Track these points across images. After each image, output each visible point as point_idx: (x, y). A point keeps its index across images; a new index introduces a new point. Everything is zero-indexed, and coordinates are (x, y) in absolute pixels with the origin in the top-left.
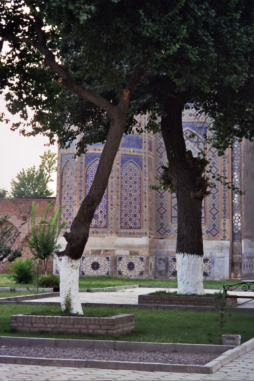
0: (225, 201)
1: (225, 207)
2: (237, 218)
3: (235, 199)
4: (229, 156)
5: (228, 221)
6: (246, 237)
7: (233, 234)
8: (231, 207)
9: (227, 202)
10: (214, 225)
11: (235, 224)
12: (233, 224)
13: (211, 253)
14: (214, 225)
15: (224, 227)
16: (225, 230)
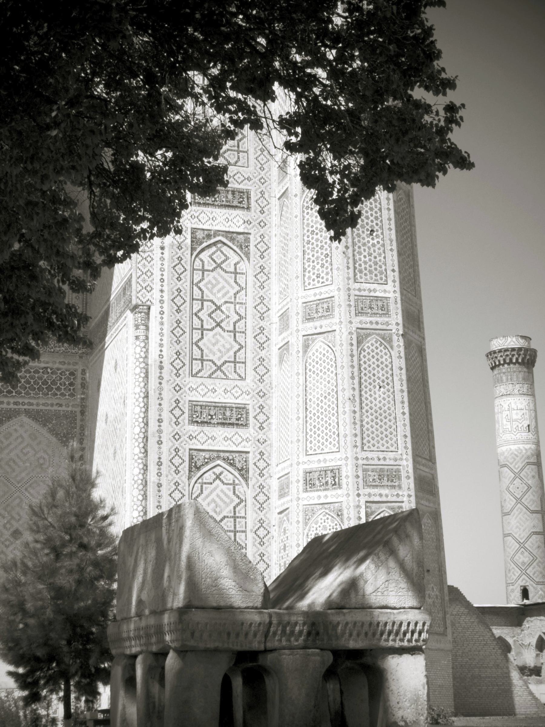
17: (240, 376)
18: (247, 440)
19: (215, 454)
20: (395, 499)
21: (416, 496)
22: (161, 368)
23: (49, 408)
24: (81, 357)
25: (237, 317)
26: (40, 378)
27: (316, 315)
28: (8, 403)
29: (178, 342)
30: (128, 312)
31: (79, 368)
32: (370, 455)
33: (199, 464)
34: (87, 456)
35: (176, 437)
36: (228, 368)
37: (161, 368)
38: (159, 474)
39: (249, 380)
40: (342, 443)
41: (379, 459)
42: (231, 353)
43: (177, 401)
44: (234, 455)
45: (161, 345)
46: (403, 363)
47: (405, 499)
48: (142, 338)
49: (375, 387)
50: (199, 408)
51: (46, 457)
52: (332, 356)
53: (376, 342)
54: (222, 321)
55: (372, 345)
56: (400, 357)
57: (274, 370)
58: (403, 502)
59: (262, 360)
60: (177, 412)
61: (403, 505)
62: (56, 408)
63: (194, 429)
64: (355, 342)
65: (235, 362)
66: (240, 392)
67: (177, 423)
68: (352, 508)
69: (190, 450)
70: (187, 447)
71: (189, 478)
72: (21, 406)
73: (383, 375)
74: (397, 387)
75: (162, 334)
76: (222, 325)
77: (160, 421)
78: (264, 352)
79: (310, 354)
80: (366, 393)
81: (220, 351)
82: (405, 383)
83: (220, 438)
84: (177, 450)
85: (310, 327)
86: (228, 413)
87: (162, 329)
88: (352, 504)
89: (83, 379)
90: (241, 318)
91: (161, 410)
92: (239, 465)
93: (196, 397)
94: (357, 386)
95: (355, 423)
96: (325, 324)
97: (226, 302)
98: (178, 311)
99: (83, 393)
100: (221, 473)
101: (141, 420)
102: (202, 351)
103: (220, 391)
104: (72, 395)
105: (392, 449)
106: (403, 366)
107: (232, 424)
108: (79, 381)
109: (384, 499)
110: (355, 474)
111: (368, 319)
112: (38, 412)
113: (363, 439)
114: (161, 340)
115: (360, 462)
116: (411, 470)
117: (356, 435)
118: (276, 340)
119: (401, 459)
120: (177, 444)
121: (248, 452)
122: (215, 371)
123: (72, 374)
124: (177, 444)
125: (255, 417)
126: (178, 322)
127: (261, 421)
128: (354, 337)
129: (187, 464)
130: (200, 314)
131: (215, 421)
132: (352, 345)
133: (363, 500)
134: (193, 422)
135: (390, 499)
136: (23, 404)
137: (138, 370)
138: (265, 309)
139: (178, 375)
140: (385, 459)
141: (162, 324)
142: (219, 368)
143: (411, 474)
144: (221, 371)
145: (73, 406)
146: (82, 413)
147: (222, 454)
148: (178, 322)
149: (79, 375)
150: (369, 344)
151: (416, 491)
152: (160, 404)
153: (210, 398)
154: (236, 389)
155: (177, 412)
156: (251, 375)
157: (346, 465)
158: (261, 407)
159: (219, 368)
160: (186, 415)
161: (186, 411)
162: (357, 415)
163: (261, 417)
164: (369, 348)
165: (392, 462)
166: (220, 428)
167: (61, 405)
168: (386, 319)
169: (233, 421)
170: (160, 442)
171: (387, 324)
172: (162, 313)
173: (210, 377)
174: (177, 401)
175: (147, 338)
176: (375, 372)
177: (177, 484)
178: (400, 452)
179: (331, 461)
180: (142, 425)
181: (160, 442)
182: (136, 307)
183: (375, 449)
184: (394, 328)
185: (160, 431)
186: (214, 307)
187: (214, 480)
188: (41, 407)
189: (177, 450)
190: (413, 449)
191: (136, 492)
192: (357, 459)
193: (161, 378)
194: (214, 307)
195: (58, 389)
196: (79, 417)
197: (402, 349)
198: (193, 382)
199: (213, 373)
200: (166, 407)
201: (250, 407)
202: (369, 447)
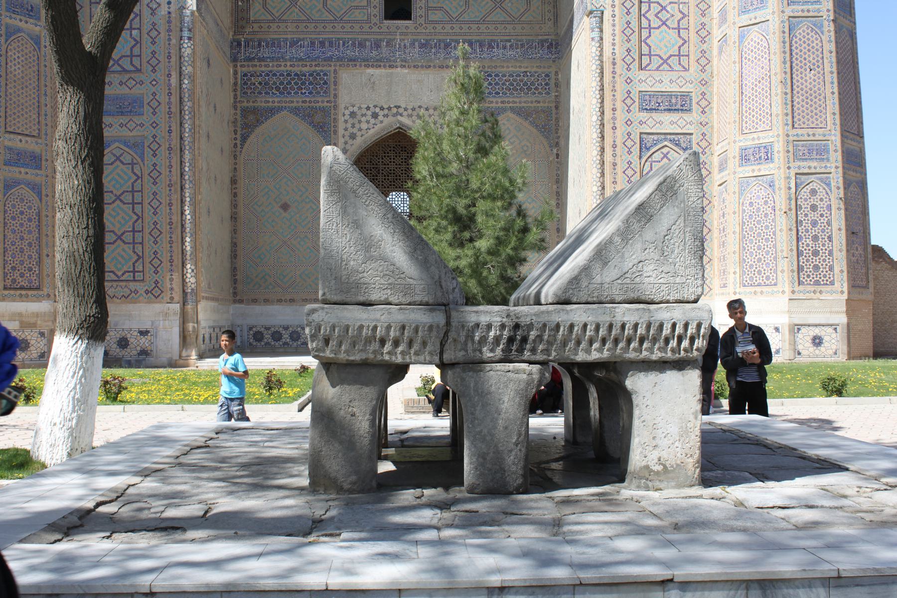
0: (171, 247)
1: (171, 256)
2: (189, 271)
3: (187, 244)
4: (176, 183)
5: (176, 276)
6: (207, 298)
7: (184, 293)
8: (180, 256)
9: (174, 248)
10: (156, 282)
11: (187, 280)
12: (184, 280)
13: (153, 322)
14: (156, 282)
15: (171, 284)
16: (172, 289)
17: (683, 67)
18: (691, 123)
19: (663, 137)
20: (823, 170)
21: (844, 167)
22: (614, 64)
23: (530, 105)
24: (554, 61)
25: (681, 16)
26: (521, 81)
27: (751, 8)
28: (497, 103)
29: (628, 41)
30: (585, 17)
31: (553, 70)
32: (800, 132)
33: (648, 145)
34: (562, 143)
35: (629, 122)
36: (674, 61)
37: (614, 64)
38: (614, 155)
39: (692, 70)
40: (774, 122)
41: (809, 136)
42: (676, 48)
43: (629, 92)
44: (679, 137)
45: (614, 44)
46: (833, 47)
47: (833, 170)
48: (597, 39)
49: (806, 70)
50: (647, 97)
51: (529, 144)
52: (766, 44)
53: (808, 29)
54: (667, 20)
55: (804, 31)
56: (830, 41)
57: (715, 61)
59: (703, 52)
60: (629, 101)
62: (535, 104)
63: (644, 115)
64: (787, 30)
65: (679, 55)
66: (684, 82)
67: (629, 111)
69: (641, 133)
70: (638, 132)
71: (640, 158)
72: (506, 105)
73: (814, 59)
74: (827, 69)
75: (614, 35)
76: (667, 23)
77: (614, 110)
78: (705, 45)
79: (746, 43)
80: (797, 75)
81: (666, 46)
82: (834, 65)
83: (668, 123)
84: (629, 134)
85: (745, 19)
86: (674, 101)
87: (614, 30)
88: (783, 176)
89: (557, 79)
90: (684, 16)
91: (614, 100)
92: (684, 145)
93: (644, 87)
94: (788, 70)
95: (786, 104)
96: (760, 15)
97: (670, 3)
98: (628, 13)
99: (557, 91)
100: (668, 153)
101: (598, 109)
102: (650, 47)
103: (666, 81)
104: (548, 93)
105: (821, 126)
106: (834, 49)
107: (678, 110)
108: (552, 82)
109: (813, 171)
111: (800, 8)
112: (521, 108)
113: (793, 117)
114: (614, 40)
115: (791, 138)
116: (839, 144)
117: (787, 115)
118: (717, 34)
119: (830, 135)
120: (629, 129)
121: (691, 134)
122: (662, 64)
123: (547, 75)
124: (629, 129)
125: (698, 103)
126: (628, 23)
127: (703, 106)
128: (787, 25)
129: (638, 145)
130: (647, 15)
131: (662, 108)
132: (784, 32)
134: (642, 109)
135: (818, 170)
136: (509, 102)
137: (594, 67)
138: (706, 7)
139: (629, 69)
140: (814, 135)
141: (614, 25)
142: (665, 61)
144: (668, 64)
145: (549, 102)
146: (557, 108)
147: (669, 137)
148: (628, 23)
149: (553, 76)
150: (801, 31)
151: (843, 162)
152: (614, 95)
153: (658, 88)
154: (681, 79)
155: (629, 101)
156: (694, 68)
157: (778, 141)
158: (703, 94)
159: (665, 61)
160: (637, 103)
161: (637, 100)
162: (789, 96)
163: (704, 103)
164: (800, 34)
165: (821, 138)
166: (666, 113)
167: (539, 102)
168: (817, 6)
169: (678, 107)
170: (614, 128)
171: (819, 11)
172: (614, 16)
173: (657, 69)
174: (629, 92)
175: (602, 39)
176: (806, 56)
177: (630, 163)
178: (829, 128)
179: (765, 138)
180: (599, 114)
181: (614, 128)
182: (591, 12)
184: (824, 14)
185: (614, 119)
186: (660, 8)
187: (662, 159)
188: (523, 105)
189: (629, 134)
191: (595, 171)
192: (788, 135)
193: (614, 72)
194: (660, 8)
195: (536, 89)
196: (554, 111)
197: (832, 34)
198: (643, 75)
199: (660, 66)
200: (620, 96)
201: (693, 94)
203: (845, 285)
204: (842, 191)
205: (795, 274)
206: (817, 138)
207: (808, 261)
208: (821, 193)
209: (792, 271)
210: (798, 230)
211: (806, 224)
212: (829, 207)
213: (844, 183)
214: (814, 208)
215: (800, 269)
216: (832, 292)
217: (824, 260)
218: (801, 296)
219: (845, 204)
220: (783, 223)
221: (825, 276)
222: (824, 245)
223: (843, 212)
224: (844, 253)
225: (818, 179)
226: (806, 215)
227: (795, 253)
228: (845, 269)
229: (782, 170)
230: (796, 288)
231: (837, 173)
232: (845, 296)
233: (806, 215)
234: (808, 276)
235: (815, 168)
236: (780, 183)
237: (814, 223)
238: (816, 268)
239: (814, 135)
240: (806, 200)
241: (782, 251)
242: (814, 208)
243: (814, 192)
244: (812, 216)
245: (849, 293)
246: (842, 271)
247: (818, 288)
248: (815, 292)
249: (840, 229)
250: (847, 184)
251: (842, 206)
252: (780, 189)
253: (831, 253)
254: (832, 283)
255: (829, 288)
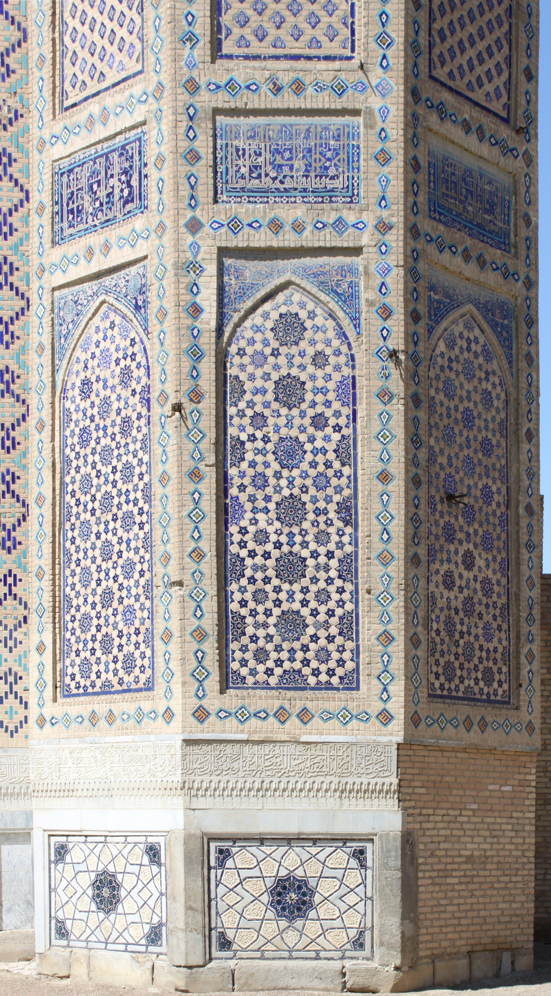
20: (328, 239)
21: (413, 231)
32: (241, 71)
40: (150, 33)
41: (277, 89)
47: (366, 239)
58: (357, 251)
61: (358, 261)
68: (171, 273)
88: (169, 261)
105: (333, 48)
109: (289, 239)
110: (184, 145)
115: (206, 100)
116: (396, 130)
119: (362, 87)
133: (208, 245)
135: (309, 238)
143: (396, 146)
151: (412, 209)
165: (324, 101)
178: (359, 56)
183: (264, 48)
190: (412, 47)
192: (192, 87)
202: (242, 41)
203: (398, 689)
204: (397, 325)
205: (210, 647)
206: (312, 99)
207: (259, 596)
208: (321, 332)
209: (200, 635)
210: (223, 481)
211: (258, 457)
212: (349, 390)
213: (411, 294)
214: (289, 391)
215: (228, 627)
216: (346, 717)
217: (323, 597)
218: (231, 730)
219: (412, 377)
220: (169, 453)
221: (323, 655)
222: (322, 538)
223: (397, 409)
224: (397, 569)
225: (307, 273)
226: (259, 420)
227: (209, 566)
228: (397, 627)
229: (168, 239)
230: (214, 701)
231: (382, 249)
232: (396, 732)
233: (259, 420)
234: (261, 655)
235: (298, 227)
236: (164, 295)
237: (289, 453)
238: (292, 623)
239: (298, 87)
240: (259, 359)
241: (167, 558)
242: (289, 391)
243: (290, 328)
244: (283, 423)
245: (413, 720)
246: (386, 638)
247: (297, 701)
248: (281, 715)
249: (384, 477)
250: (427, 305)
251: (397, 385)
252: (163, 313)
253: (348, 569)
254: (351, 683)
255: (334, 701)
